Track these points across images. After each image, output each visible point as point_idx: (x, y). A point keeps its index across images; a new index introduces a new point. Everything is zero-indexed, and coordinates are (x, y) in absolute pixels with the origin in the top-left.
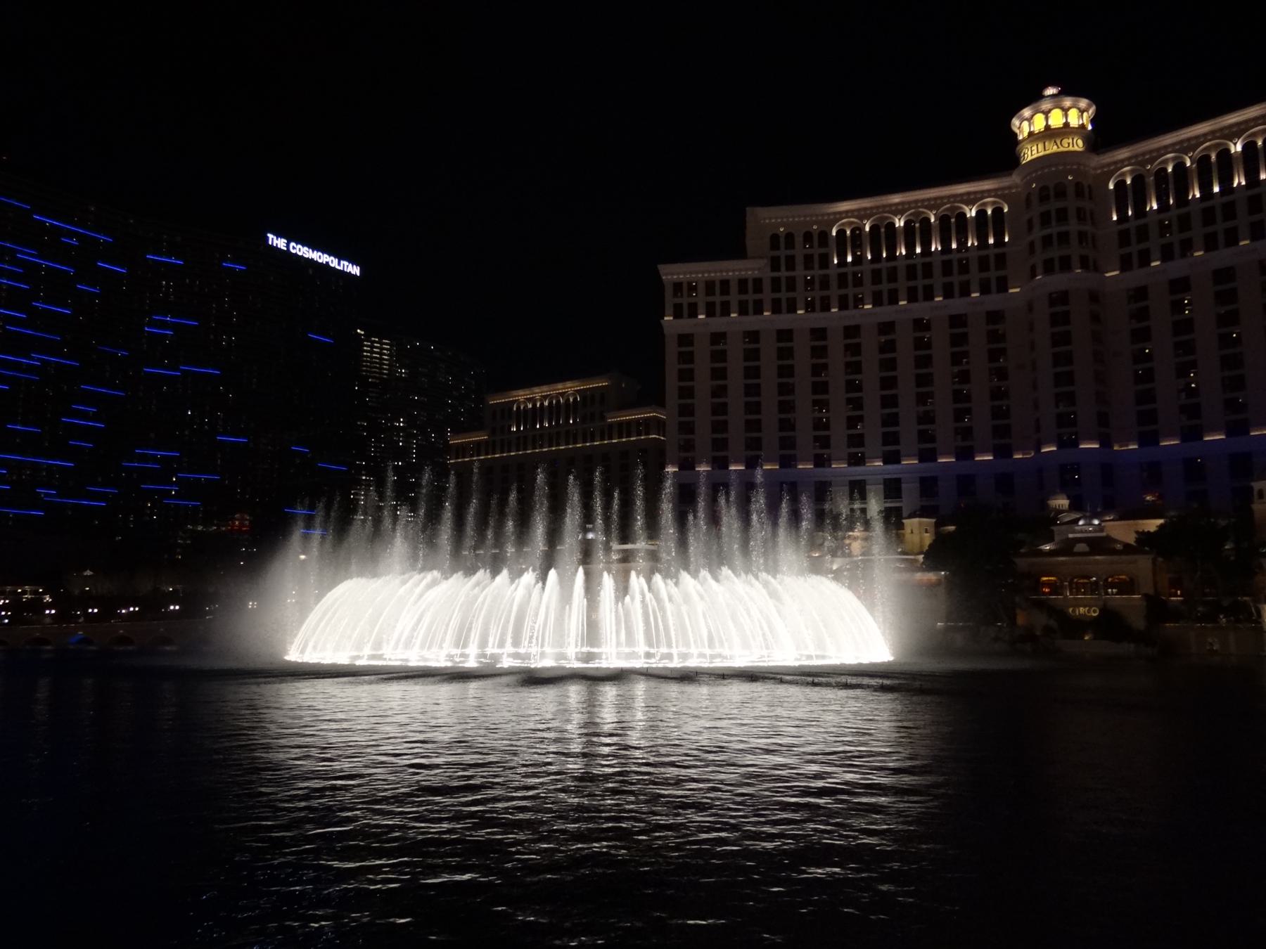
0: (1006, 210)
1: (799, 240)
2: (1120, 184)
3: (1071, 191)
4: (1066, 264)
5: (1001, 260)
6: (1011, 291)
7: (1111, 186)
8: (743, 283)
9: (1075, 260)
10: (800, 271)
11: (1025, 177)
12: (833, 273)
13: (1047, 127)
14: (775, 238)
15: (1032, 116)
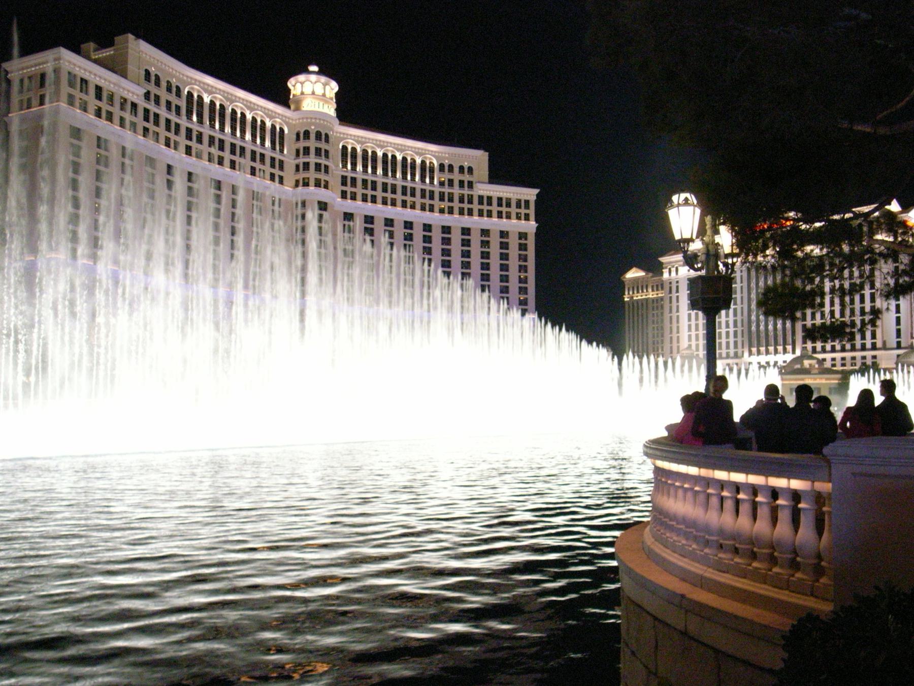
0: (286, 131)
1: (164, 84)
2: (345, 148)
3: (331, 140)
4: (326, 187)
5: (281, 163)
6: (286, 188)
7: (341, 147)
8: (124, 101)
9: (330, 187)
10: (163, 113)
11: (303, 118)
12: (184, 122)
13: (324, 95)
14: (148, 73)
15: (316, 82)
